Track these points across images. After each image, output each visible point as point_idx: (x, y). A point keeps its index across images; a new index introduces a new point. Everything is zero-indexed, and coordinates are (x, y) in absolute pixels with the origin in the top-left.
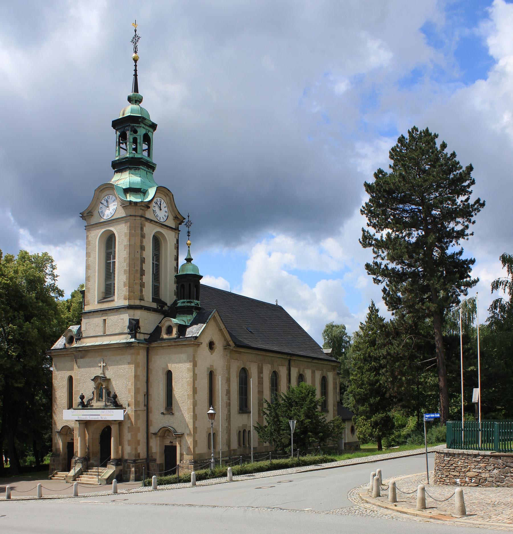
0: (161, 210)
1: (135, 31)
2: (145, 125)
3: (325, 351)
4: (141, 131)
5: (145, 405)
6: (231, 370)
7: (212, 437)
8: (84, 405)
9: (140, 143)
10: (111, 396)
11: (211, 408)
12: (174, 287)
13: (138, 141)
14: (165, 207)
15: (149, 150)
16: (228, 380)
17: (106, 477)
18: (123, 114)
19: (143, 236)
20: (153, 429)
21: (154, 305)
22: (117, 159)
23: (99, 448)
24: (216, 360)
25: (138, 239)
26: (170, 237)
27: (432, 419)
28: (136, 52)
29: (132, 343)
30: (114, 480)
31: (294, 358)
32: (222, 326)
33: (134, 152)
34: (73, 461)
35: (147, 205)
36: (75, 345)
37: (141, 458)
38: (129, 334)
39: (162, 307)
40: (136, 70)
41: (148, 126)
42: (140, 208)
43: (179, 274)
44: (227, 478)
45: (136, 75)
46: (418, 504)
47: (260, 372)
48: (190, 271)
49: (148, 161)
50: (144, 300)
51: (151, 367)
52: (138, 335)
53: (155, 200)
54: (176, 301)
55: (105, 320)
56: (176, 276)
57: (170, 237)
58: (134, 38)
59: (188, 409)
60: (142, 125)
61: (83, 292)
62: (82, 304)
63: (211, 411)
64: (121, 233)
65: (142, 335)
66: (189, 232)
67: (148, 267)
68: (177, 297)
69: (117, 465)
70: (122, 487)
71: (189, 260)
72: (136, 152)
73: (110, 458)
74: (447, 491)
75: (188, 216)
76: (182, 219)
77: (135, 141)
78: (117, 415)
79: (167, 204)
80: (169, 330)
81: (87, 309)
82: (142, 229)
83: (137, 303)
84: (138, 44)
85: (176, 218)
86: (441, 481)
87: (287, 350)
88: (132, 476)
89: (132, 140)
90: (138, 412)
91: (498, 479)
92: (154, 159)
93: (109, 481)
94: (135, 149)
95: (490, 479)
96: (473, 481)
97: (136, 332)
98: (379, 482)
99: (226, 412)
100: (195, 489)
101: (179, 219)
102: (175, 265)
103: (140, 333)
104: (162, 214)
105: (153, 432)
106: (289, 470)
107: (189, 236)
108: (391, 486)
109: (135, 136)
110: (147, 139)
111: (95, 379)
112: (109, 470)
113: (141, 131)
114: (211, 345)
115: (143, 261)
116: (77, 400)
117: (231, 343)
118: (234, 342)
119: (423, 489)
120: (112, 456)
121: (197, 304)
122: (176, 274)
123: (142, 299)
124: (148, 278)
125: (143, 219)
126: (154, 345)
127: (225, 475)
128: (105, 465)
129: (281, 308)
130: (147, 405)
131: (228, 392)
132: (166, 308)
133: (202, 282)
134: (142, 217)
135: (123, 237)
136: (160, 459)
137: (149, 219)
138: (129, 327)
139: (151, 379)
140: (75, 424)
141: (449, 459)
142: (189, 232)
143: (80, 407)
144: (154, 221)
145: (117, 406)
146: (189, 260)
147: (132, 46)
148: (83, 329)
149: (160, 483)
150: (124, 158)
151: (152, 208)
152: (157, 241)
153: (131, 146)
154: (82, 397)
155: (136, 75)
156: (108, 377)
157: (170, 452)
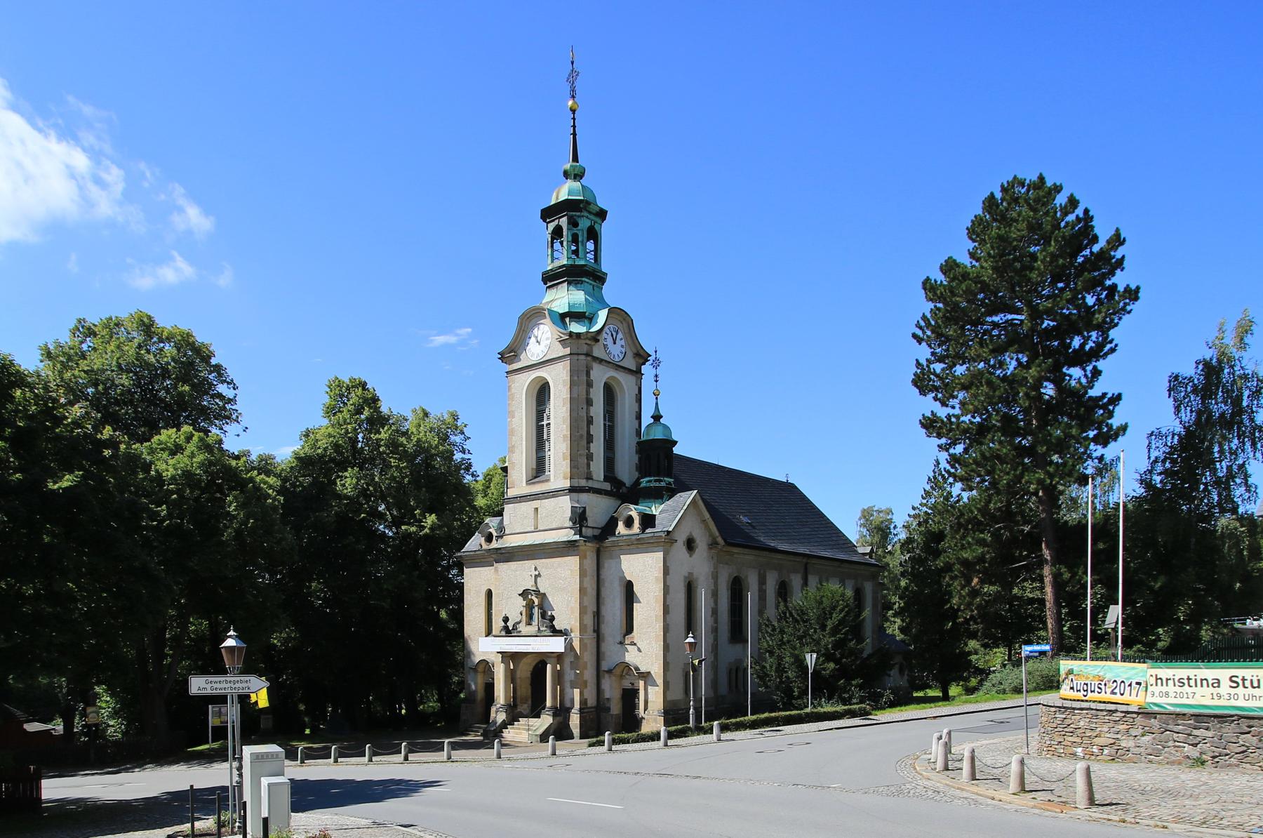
3: (861, 550)
4: (584, 224)
8: (508, 632)
12: (636, 458)
16: (715, 594)
19: (590, 384)
20: (605, 666)
21: (607, 486)
24: (700, 564)
28: (573, 97)
31: (814, 561)
32: (707, 515)
34: (493, 709)
35: (595, 337)
36: (494, 545)
44: (714, 736)
47: (762, 581)
48: (658, 434)
49: (594, 270)
53: (606, 329)
54: (638, 479)
55: (536, 509)
60: (585, 214)
61: (505, 469)
62: (504, 484)
63: (690, 640)
64: (559, 379)
67: (598, 430)
68: (640, 472)
69: (555, 715)
71: (657, 418)
77: (575, 239)
79: (624, 334)
80: (629, 522)
81: (511, 493)
82: (588, 374)
83: (583, 483)
87: (802, 550)
92: (605, 267)
93: (544, 738)
94: (576, 252)
97: (581, 526)
99: (711, 641)
100: (667, 750)
101: (642, 357)
104: (616, 350)
110: (593, 235)
111: (525, 594)
112: (545, 721)
113: (584, 224)
114: (690, 544)
115: (590, 421)
116: (498, 624)
117: (720, 540)
120: (549, 703)
123: (589, 478)
124: (598, 448)
129: (792, 487)
130: (597, 631)
131: (715, 612)
132: (624, 490)
133: (676, 450)
134: (587, 355)
135: (560, 387)
136: (616, 708)
138: (571, 519)
139: (604, 593)
145: (555, 632)
146: (657, 418)
148: (506, 523)
149: (615, 742)
151: (602, 341)
152: (610, 393)
153: (569, 247)
154: (506, 620)
157: (630, 697)
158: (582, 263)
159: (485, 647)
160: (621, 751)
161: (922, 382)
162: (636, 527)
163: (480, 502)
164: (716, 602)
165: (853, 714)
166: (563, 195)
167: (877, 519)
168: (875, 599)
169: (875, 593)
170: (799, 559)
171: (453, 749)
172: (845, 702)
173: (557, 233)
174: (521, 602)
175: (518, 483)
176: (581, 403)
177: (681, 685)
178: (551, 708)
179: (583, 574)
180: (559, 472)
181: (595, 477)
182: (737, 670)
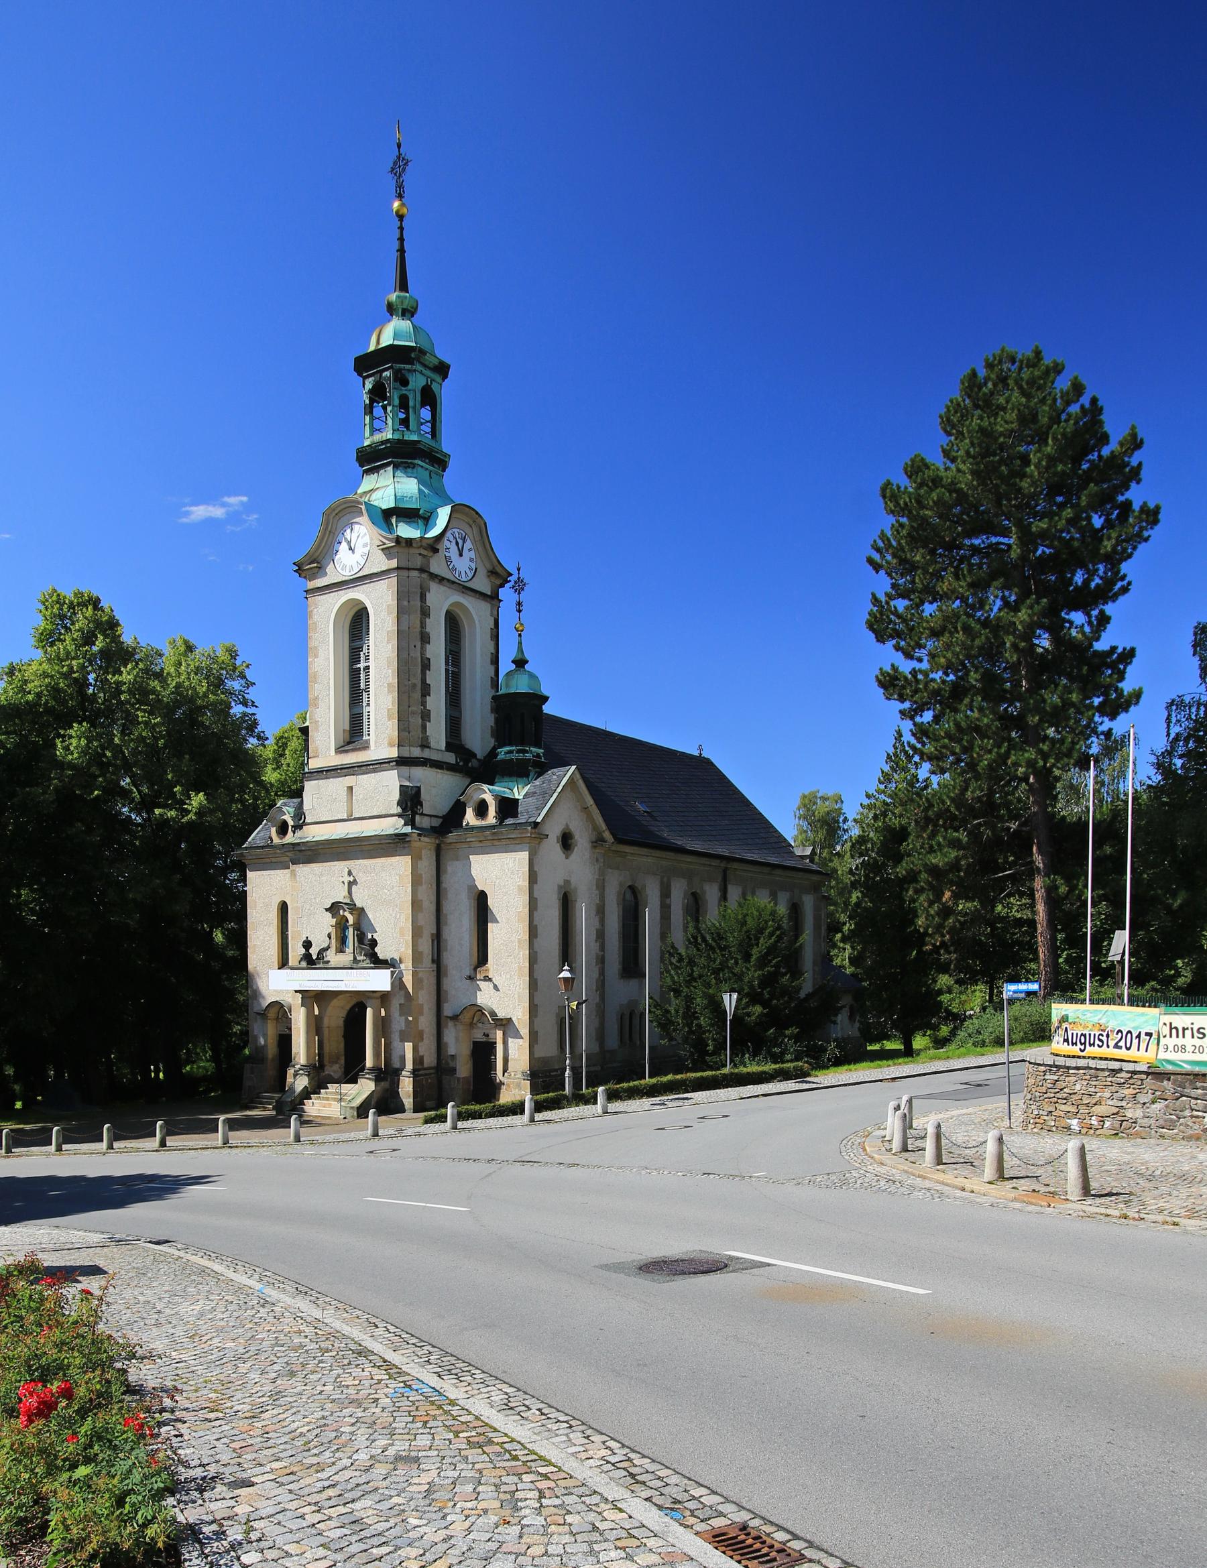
0: (461, 555)
1: (399, 146)
2: (425, 366)
3: (798, 852)
4: (417, 381)
5: (433, 961)
6: (607, 890)
7: (566, 1026)
8: (311, 962)
9: (414, 408)
10: (367, 942)
11: (566, 967)
12: (491, 719)
13: (411, 404)
14: (470, 550)
15: (434, 421)
16: (601, 911)
17: (357, 1102)
18: (378, 342)
19: (425, 613)
20: (448, 1011)
22: (367, 443)
23: (342, 1045)
24: (579, 869)
25: (416, 619)
26: (477, 613)
27: (1023, 995)
28: (400, 196)
29: (405, 834)
30: (372, 1111)
31: (735, 865)
32: (590, 801)
33: (402, 428)
34: (290, 1072)
35: (433, 546)
36: (290, 838)
37: (426, 1065)
38: (399, 816)
39: (466, 761)
40: (401, 239)
41: (430, 368)
42: (418, 551)
43: (500, 692)
44: (599, 1108)
45: (402, 251)
46: (989, 1171)
47: (665, 894)
48: (521, 685)
50: (429, 747)
51: (444, 885)
52: (417, 818)
53: (448, 534)
54: (494, 748)
55: (350, 789)
56: (493, 698)
57: (477, 613)
58: (395, 163)
59: (520, 968)
60: (419, 367)
61: (305, 731)
63: (565, 974)
65: (426, 819)
66: (519, 604)
67: (438, 678)
69: (377, 1080)
70: (388, 1124)
71: (520, 663)
72: (407, 427)
73: (364, 1066)
74: (1050, 1144)
75: (519, 570)
76: (505, 575)
77: (404, 404)
78: (379, 980)
79: (474, 542)
80: (481, 809)
81: (314, 764)
82: (423, 597)
83: (416, 752)
84: (405, 177)
85: (493, 573)
86: (1039, 1124)
88: (408, 1102)
89: (397, 402)
90: (420, 975)
91: (1161, 1122)
93: (362, 1112)
94: (405, 422)
95: (1145, 1122)
96: (1107, 1124)
97: (414, 814)
98: (907, 1123)
99: (596, 975)
100: (534, 1128)
101: (499, 576)
102: (493, 674)
103: (422, 814)
104: (463, 565)
105: (450, 1015)
106: (722, 1093)
107: (519, 611)
108: (931, 1130)
109: (404, 391)
110: (429, 398)
111: (334, 908)
112: (365, 1087)
113: (417, 381)
114: (566, 841)
115: (426, 665)
116: (296, 951)
117: (607, 835)
118: (612, 834)
119: (1000, 1140)
120: (369, 1063)
121: (538, 756)
122: (493, 693)
124: (437, 703)
125: (424, 576)
126: (452, 837)
127: (593, 1100)
128: (354, 1081)
129: (708, 763)
130: (437, 960)
131: (601, 935)
132: (474, 763)
133: (547, 709)
134: (422, 570)
135: (384, 614)
136: (464, 1069)
137: (437, 576)
138: (399, 804)
139: (447, 907)
140: (294, 997)
141: (1056, 1078)
142: (519, 604)
143: (304, 964)
144: (448, 580)
145: (378, 963)
146: (520, 663)
147: (391, 182)
149: (461, 1116)
150: (383, 443)
154: (307, 944)
155: (402, 251)
156: (359, 905)
157: (483, 1053)
158: (414, 437)
159: (277, 984)
160: (470, 1129)
161: (881, 626)
162: (491, 818)
163: (271, 776)
164: (602, 921)
165: (785, 1075)
166: (387, 339)
167: (822, 808)
168: (817, 918)
169: (817, 909)
170: (715, 862)
171: (232, 1129)
172: (776, 1059)
173: (378, 393)
174: (329, 921)
175: (324, 752)
176: (411, 640)
177: (555, 1036)
178: (372, 1070)
179: (416, 881)
180: (382, 738)
181: (433, 745)
182: (631, 1015)
